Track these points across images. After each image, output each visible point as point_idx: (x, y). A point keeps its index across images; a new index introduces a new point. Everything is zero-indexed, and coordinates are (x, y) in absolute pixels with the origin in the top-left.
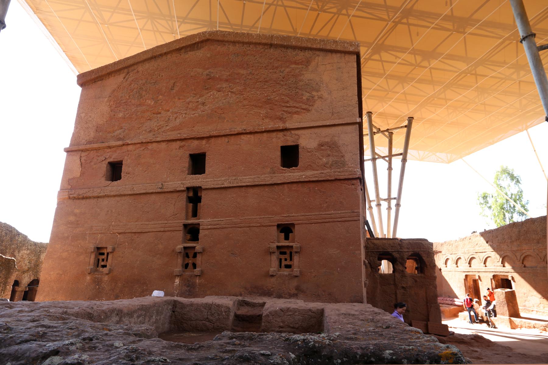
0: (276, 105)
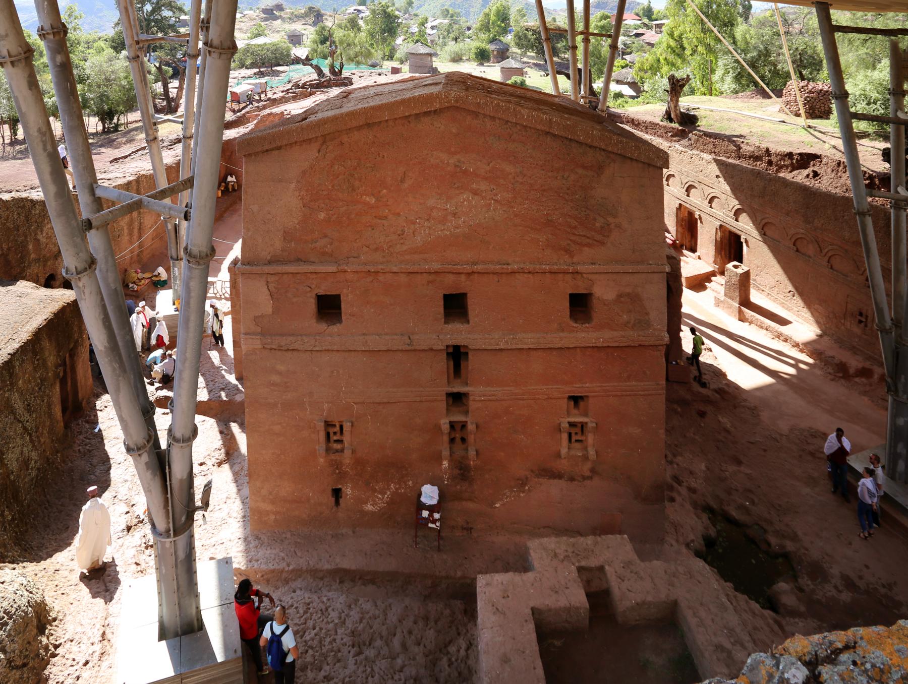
0: (559, 229)
